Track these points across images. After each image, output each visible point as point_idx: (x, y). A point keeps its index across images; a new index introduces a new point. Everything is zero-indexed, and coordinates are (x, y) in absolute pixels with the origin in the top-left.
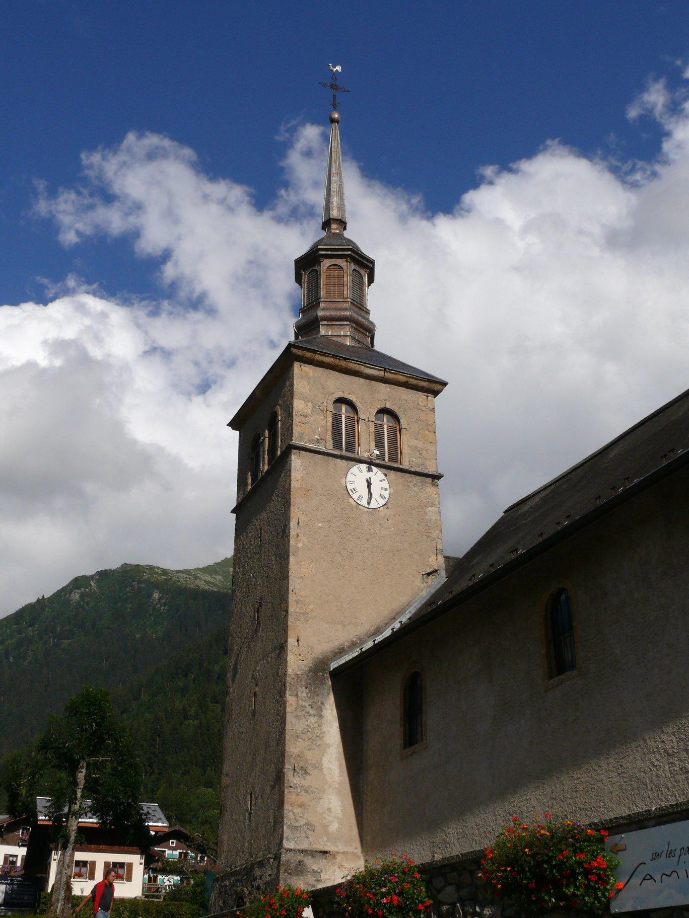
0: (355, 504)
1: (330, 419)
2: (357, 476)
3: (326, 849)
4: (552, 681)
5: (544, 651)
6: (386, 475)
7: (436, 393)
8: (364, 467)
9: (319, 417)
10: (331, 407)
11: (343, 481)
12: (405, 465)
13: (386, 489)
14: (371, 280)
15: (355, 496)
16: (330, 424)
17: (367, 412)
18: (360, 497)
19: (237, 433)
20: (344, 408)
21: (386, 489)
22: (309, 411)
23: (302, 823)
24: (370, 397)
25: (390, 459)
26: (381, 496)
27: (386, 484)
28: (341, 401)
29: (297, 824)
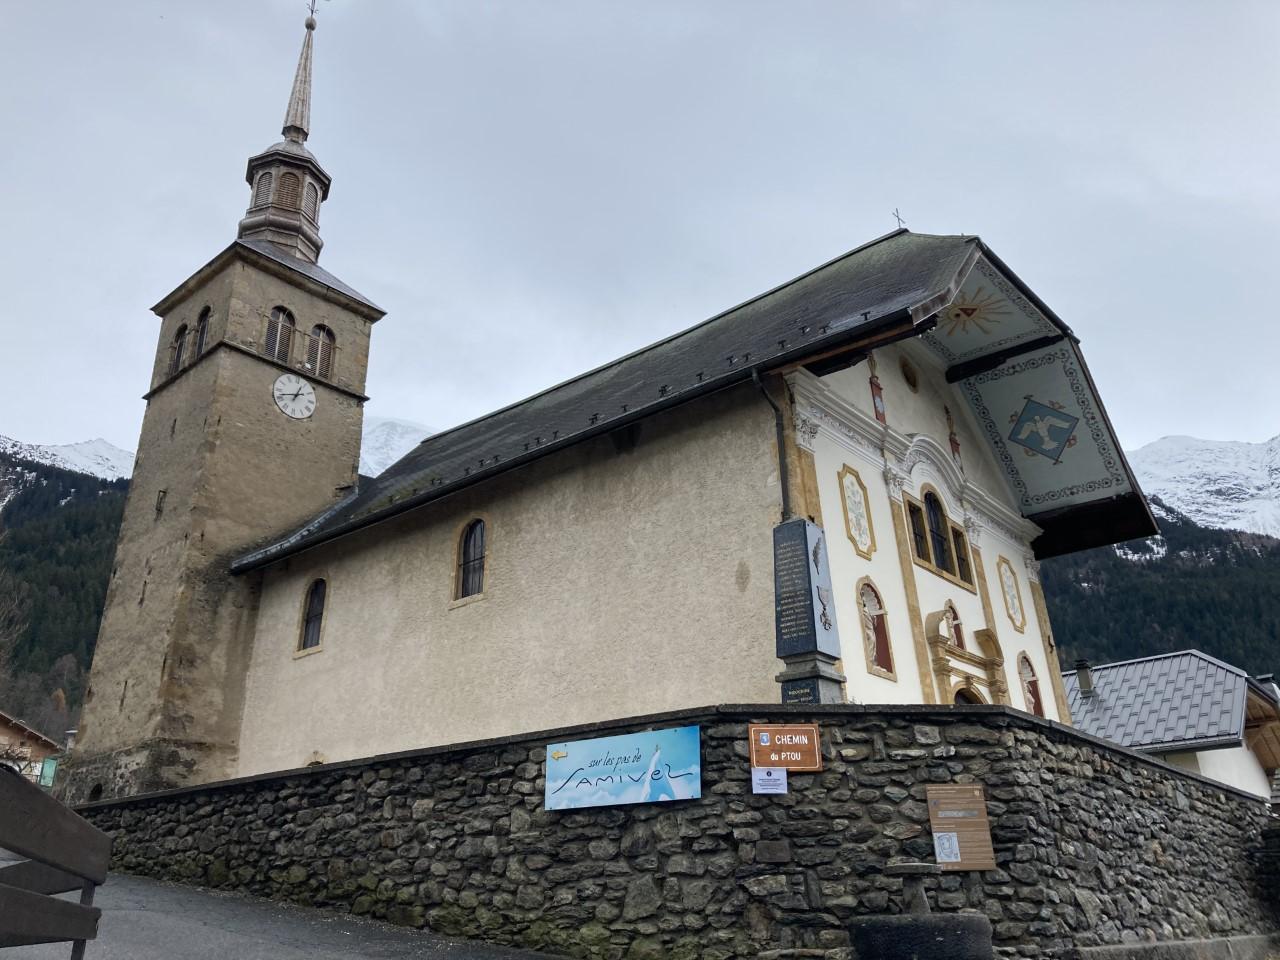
0: (279, 411)
1: (266, 325)
2: (287, 384)
3: (203, 741)
4: (457, 601)
5: (453, 574)
6: (314, 389)
7: (374, 320)
8: (293, 377)
9: (256, 321)
10: (269, 313)
11: (271, 387)
12: (334, 382)
13: (312, 403)
14: (325, 197)
15: (281, 404)
16: (265, 330)
17: (305, 324)
18: (286, 406)
19: (161, 319)
20: (282, 317)
21: (312, 403)
22: (246, 313)
23: (181, 713)
24: (308, 312)
25: (320, 374)
26: (308, 409)
27: (313, 397)
28: (280, 309)
29: (176, 716)
